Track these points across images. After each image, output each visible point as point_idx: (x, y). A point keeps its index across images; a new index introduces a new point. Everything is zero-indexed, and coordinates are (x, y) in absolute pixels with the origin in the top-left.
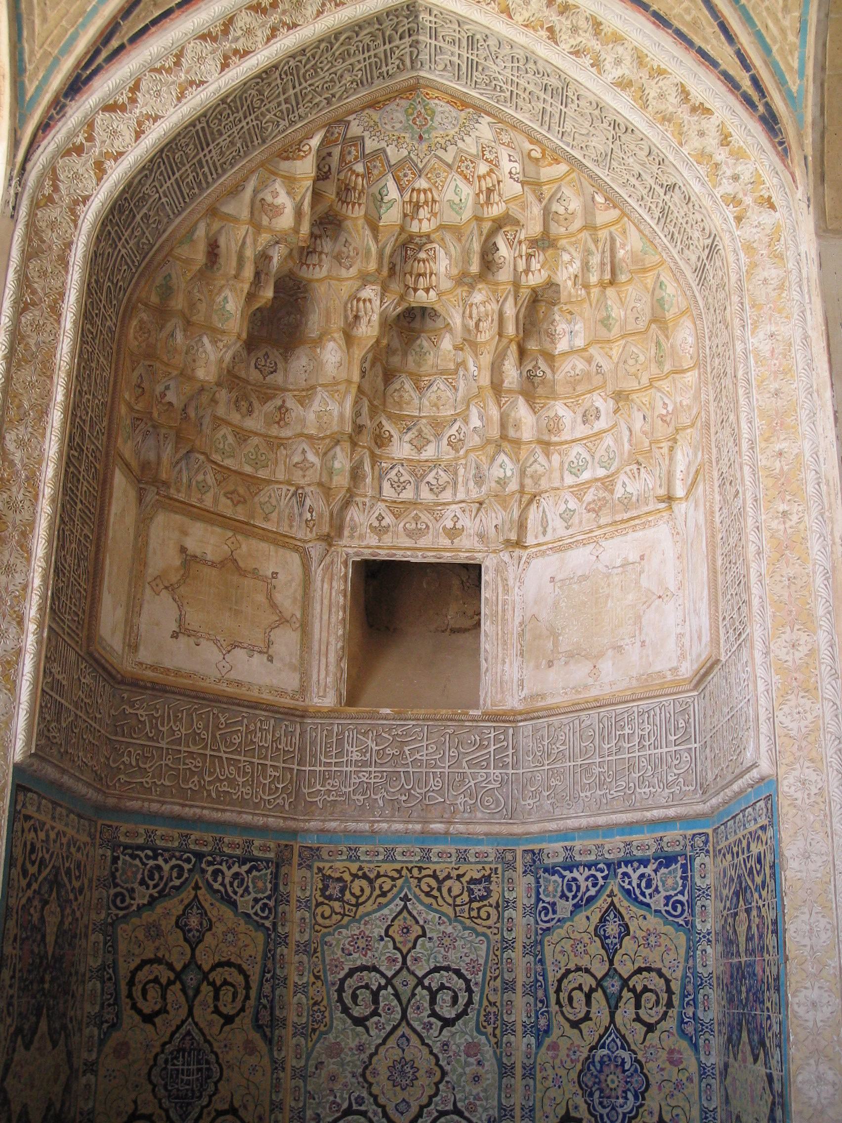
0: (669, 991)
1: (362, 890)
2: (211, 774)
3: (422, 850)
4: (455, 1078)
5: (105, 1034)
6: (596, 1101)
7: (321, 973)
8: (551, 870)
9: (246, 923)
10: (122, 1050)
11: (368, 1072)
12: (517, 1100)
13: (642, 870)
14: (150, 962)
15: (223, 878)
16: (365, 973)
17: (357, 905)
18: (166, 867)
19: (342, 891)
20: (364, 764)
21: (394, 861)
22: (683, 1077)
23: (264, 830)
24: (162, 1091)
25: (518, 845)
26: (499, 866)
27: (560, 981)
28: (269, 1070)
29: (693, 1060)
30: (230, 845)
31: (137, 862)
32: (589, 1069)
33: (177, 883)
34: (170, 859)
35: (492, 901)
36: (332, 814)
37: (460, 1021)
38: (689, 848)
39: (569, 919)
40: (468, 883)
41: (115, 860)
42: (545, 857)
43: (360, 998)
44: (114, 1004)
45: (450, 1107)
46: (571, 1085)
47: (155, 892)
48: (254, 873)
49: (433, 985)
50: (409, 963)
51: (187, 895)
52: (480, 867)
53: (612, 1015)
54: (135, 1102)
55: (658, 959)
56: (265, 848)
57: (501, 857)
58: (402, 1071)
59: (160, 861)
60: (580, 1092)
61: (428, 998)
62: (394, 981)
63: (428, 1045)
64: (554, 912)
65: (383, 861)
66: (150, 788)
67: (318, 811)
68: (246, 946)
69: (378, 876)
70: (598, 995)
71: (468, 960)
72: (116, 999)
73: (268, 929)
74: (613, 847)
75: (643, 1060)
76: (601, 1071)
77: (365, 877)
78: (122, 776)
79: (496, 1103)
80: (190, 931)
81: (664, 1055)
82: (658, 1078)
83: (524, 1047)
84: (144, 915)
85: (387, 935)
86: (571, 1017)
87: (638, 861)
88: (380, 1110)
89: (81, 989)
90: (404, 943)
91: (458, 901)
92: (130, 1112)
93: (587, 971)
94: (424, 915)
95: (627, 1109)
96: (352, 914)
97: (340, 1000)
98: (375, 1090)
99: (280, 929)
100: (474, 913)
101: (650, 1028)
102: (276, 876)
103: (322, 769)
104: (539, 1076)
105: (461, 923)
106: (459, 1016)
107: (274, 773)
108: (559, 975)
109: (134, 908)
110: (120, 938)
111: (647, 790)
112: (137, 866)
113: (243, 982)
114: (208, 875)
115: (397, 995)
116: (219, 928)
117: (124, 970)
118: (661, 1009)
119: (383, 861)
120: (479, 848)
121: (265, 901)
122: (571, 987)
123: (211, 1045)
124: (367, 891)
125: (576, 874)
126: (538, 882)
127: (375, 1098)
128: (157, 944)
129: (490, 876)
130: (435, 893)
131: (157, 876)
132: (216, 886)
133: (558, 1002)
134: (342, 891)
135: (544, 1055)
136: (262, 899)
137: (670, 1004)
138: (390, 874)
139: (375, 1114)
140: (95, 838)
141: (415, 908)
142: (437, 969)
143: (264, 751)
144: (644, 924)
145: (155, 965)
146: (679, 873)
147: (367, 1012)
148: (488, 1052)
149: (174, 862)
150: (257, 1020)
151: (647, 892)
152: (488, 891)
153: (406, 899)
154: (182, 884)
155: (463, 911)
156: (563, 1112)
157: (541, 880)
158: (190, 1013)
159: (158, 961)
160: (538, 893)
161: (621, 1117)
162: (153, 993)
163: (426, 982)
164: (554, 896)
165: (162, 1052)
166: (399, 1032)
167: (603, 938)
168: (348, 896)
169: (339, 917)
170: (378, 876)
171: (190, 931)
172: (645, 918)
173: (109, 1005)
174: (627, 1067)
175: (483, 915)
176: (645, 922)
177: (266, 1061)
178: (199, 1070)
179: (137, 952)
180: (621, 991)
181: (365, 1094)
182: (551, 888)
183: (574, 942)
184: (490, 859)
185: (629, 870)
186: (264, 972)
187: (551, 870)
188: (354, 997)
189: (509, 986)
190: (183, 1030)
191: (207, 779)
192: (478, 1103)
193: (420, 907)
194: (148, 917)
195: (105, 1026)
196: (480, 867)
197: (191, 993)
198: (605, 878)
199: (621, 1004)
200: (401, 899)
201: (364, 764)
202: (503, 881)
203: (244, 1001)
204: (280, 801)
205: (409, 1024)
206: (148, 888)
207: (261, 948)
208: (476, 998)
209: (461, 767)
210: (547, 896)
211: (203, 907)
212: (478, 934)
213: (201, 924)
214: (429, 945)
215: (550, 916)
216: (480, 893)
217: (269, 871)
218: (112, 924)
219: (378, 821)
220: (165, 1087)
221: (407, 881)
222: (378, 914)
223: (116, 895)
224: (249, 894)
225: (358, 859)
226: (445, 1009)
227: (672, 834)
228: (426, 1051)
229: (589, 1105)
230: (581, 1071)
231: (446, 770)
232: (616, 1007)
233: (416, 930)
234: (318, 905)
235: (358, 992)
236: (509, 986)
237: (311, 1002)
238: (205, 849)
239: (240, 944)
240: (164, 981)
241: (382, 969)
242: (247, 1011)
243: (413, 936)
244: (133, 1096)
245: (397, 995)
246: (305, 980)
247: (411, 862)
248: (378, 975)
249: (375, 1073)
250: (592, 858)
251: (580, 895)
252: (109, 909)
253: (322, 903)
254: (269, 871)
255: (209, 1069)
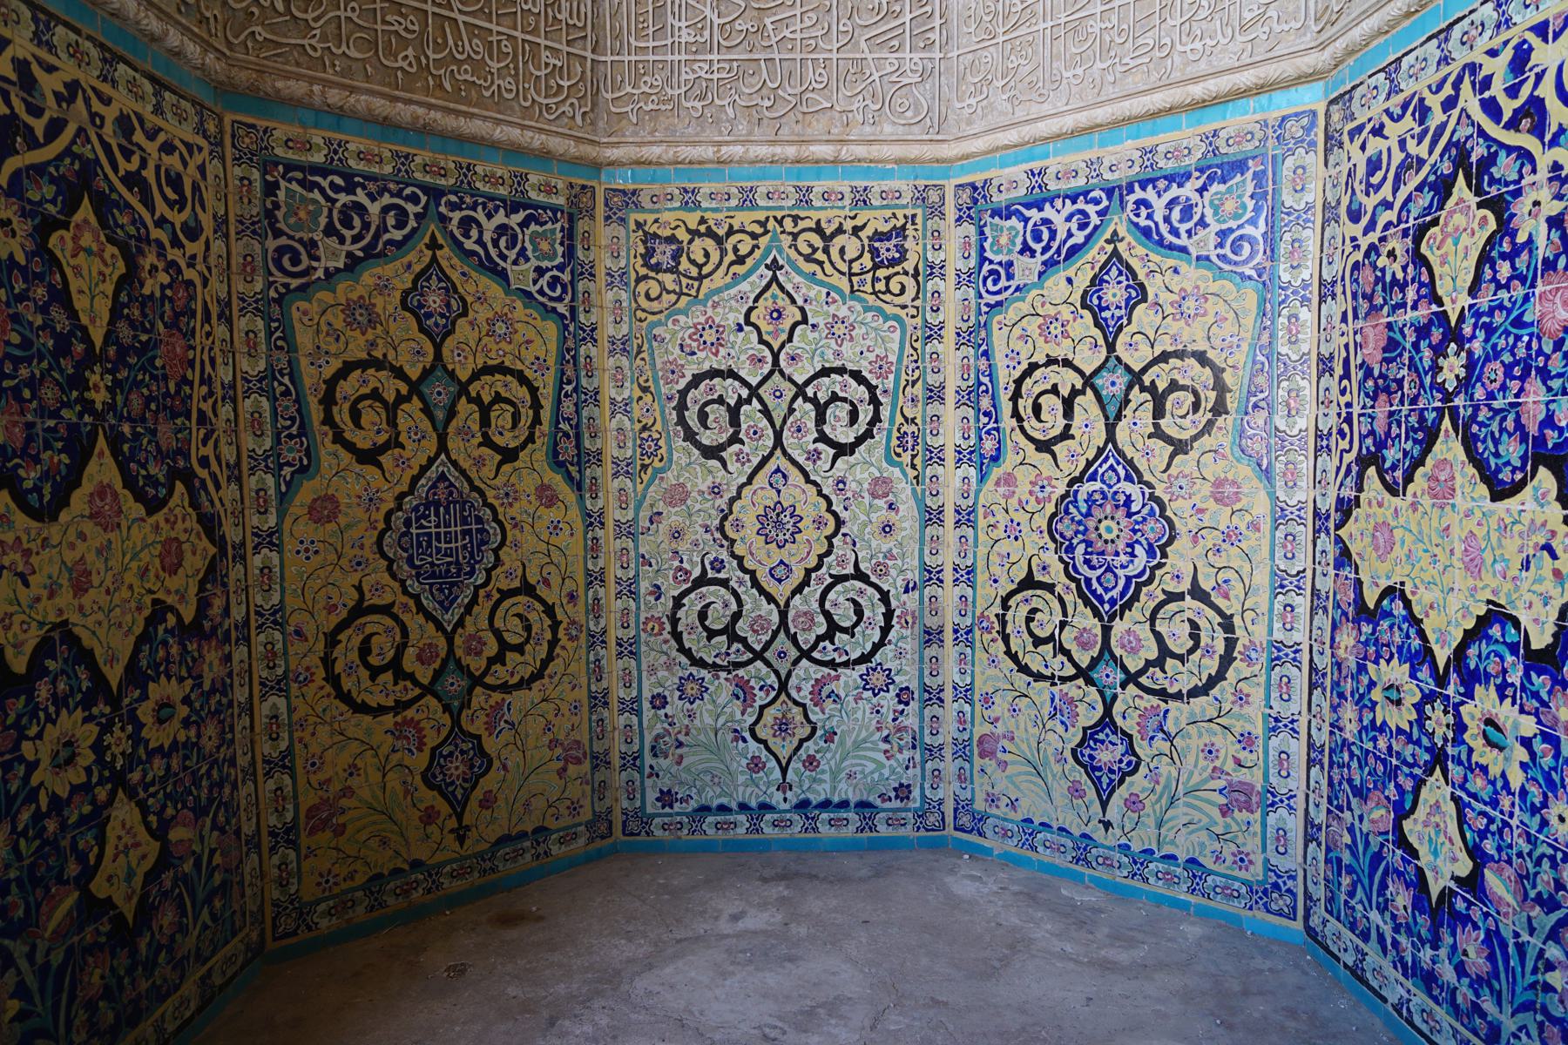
0: (1220, 387)
1: (707, 255)
2: (438, 48)
3: (798, 189)
4: (855, 528)
5: (288, 484)
6: (1079, 559)
7: (650, 383)
8: (1005, 213)
9: (525, 307)
10: (324, 510)
11: (727, 524)
12: (948, 558)
13: (1175, 191)
14: (363, 365)
15: (481, 233)
16: (717, 380)
17: (701, 278)
18: (374, 209)
19: (676, 256)
20: (701, 48)
21: (755, 207)
22: (1241, 522)
23: (545, 157)
24: (406, 567)
25: (948, 178)
26: (919, 211)
27: (1019, 382)
28: (579, 526)
29: (1263, 495)
30: (486, 178)
31: (316, 195)
32: (1067, 512)
33: (398, 235)
34: (381, 195)
35: (909, 266)
36: (652, 133)
37: (862, 447)
38: (1271, 143)
39: (1034, 286)
40: (870, 239)
41: (271, 189)
42: (993, 190)
43: (711, 418)
44: (299, 435)
45: (850, 570)
46: (1035, 536)
47: (357, 249)
48: (533, 227)
49: (819, 395)
50: (783, 364)
51: (418, 257)
52: (888, 213)
53: (1111, 429)
54: (359, 588)
55: (1200, 335)
56: (550, 190)
57: (921, 198)
58: (777, 522)
59: (361, 196)
60: (1052, 546)
61: (813, 414)
62: (761, 391)
63: (815, 483)
64: (1010, 277)
65: (737, 208)
66: (322, 58)
67: (632, 128)
68: (529, 342)
69: (731, 232)
70: (1087, 401)
71: (872, 357)
72: (302, 426)
73: (562, 316)
74: (1119, 158)
75: (1166, 498)
76: (1089, 514)
77: (710, 233)
78: (258, 29)
79: (916, 563)
80: (429, 315)
81: (1207, 489)
82: (1193, 524)
83: (958, 483)
84: (341, 287)
85: (748, 322)
86: (1038, 436)
87: (1165, 178)
88: (747, 577)
89: (226, 411)
90: (776, 334)
91: (856, 268)
92: (351, 604)
93: (1067, 363)
94: (804, 290)
95: (1133, 570)
96: (693, 292)
97: (682, 421)
98: (739, 549)
99: (582, 317)
100: (881, 286)
101: (1180, 447)
102: (569, 234)
103: (633, 58)
104: (982, 523)
105: (860, 300)
106: (860, 440)
107: (553, 61)
108: (1017, 374)
109: (320, 273)
110: (297, 325)
111: (1198, 45)
112: (315, 202)
113: (528, 397)
114: (453, 226)
115: (766, 412)
116: (481, 313)
117: (312, 377)
118: (1203, 417)
119: (737, 208)
120: (887, 185)
121: (555, 273)
122: (1037, 390)
123: (482, 494)
124: (715, 256)
125: (1049, 212)
126: (982, 233)
127: (740, 559)
128: (370, 335)
129: (904, 228)
130: (820, 256)
131: (357, 222)
132: (469, 245)
133: (1016, 414)
134: (676, 256)
135: (990, 494)
136: (548, 270)
137: (1219, 409)
138: (748, 229)
139: (741, 583)
140: (221, 144)
141: (790, 281)
142: (825, 372)
143: (532, 19)
144: (1175, 282)
145: (371, 371)
146: (1250, 188)
147: (723, 438)
148: (904, 491)
149: (387, 199)
150: (556, 454)
151: (1183, 228)
152: (903, 252)
153: (775, 266)
154: (407, 238)
155: (863, 282)
156: (1023, 575)
157: (987, 230)
158: (443, 447)
159: (379, 364)
160: (982, 249)
161: (1122, 582)
162: (372, 416)
163: (810, 391)
164: (1010, 252)
165: (399, 508)
166: (771, 466)
167: (1097, 312)
168: (684, 264)
169: (673, 297)
170: (731, 232)
171: (429, 315)
172: (1176, 271)
173: (290, 436)
174: (1135, 508)
175: (895, 288)
176: (1177, 278)
177: (574, 514)
178: (464, 533)
179: (333, 349)
180: (1130, 387)
181: (724, 555)
182: (1004, 240)
183: (1046, 319)
184: (904, 201)
185: (1150, 195)
186: (562, 382)
187: (1005, 213)
188: (703, 417)
189: (935, 394)
190: (432, 473)
191: (432, 56)
192: (890, 563)
193: (798, 279)
194: (345, 290)
195: (287, 471)
196: (888, 213)
197: (440, 415)
198: (1100, 213)
199: (1128, 412)
200: (767, 267)
201: (701, 48)
202: (925, 237)
203: (532, 426)
204: (566, 108)
205: (785, 453)
206: (342, 240)
207: (553, 347)
208: (885, 413)
209: (856, 48)
210: (996, 253)
211: (448, 278)
212: (887, 318)
213: (448, 305)
214: (811, 335)
215: (1003, 283)
216: (890, 255)
217: (558, 226)
218: (279, 301)
219: (727, 143)
220: (410, 561)
221: (775, 239)
222: (733, 291)
223: (280, 251)
224: (527, 260)
225: (697, 205)
226: (839, 430)
227: (1236, 121)
228: (812, 490)
229: (1066, 564)
230: (1054, 515)
231: (834, 56)
232: (1119, 417)
233: (793, 314)
234: (639, 280)
235: (707, 409)
236: (935, 394)
237: (638, 426)
238: (443, 182)
239: (518, 338)
240: (390, 397)
241: (742, 374)
242: (539, 442)
243: (786, 324)
244: (354, 579)
245: (766, 412)
246: (626, 394)
247: (781, 208)
248: (737, 383)
249: (738, 526)
250: (1080, 182)
251: (1055, 245)
252: (271, 274)
253: (646, 277)
254: (558, 226)
255: (482, 531)
